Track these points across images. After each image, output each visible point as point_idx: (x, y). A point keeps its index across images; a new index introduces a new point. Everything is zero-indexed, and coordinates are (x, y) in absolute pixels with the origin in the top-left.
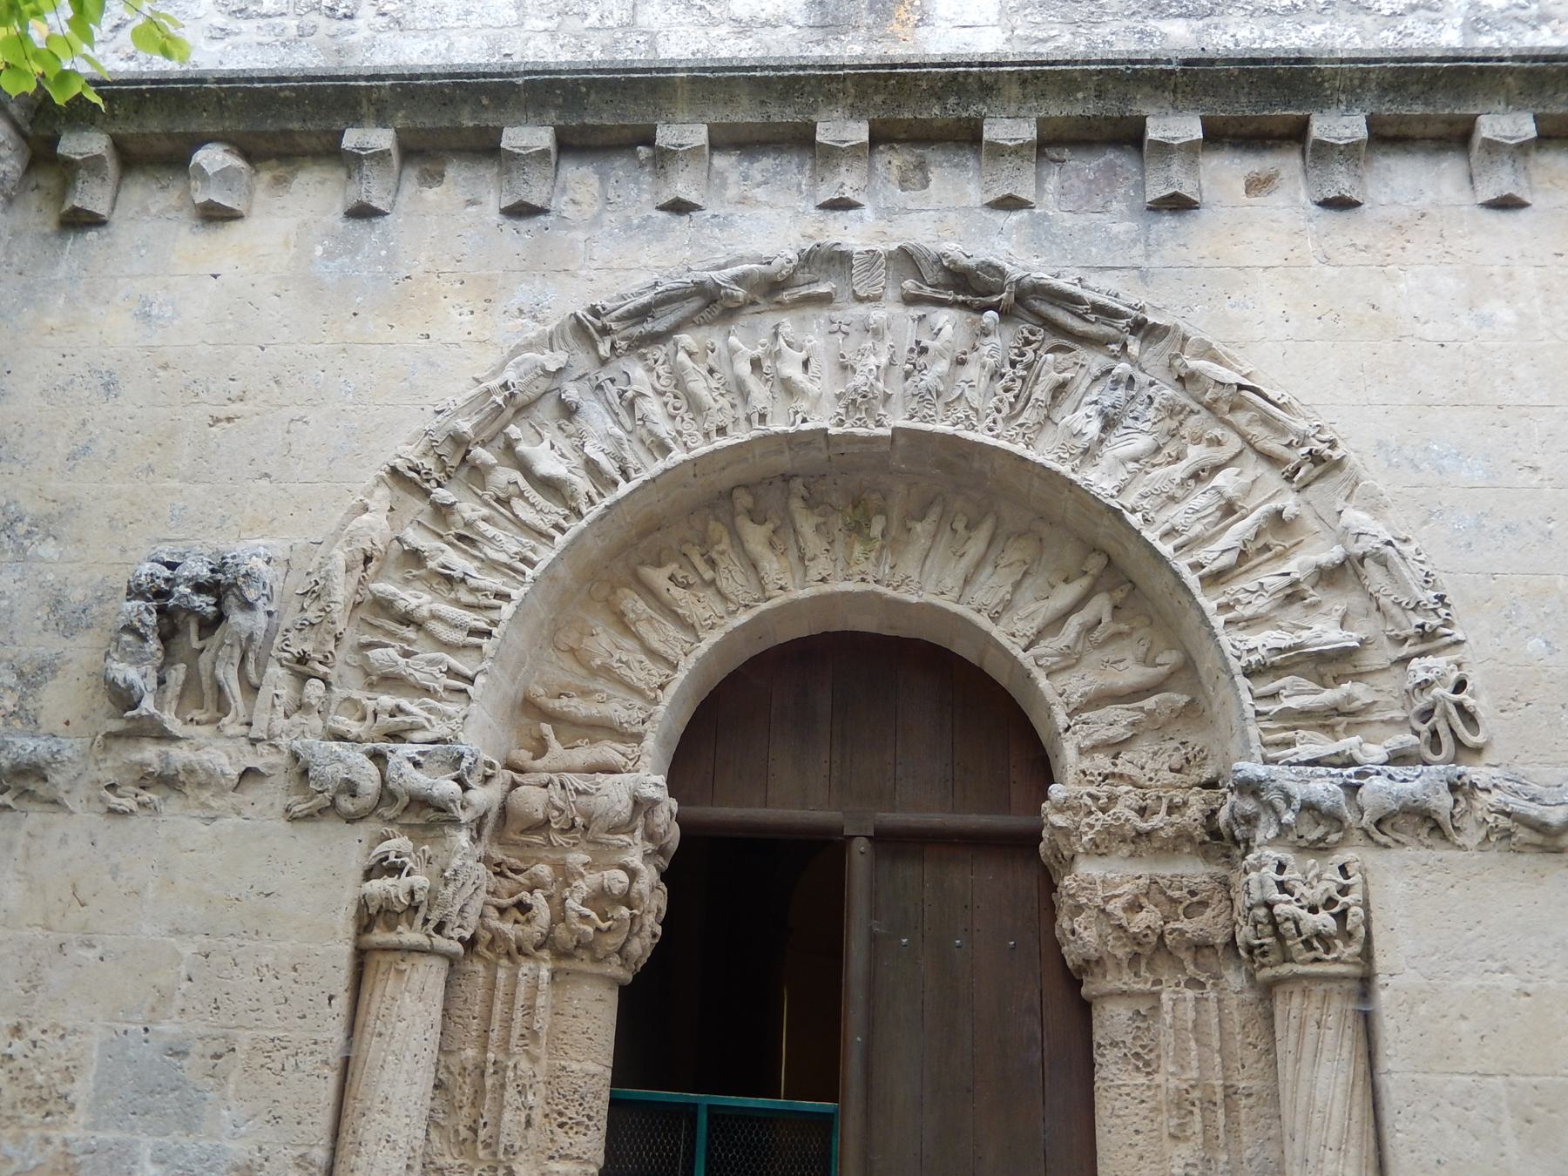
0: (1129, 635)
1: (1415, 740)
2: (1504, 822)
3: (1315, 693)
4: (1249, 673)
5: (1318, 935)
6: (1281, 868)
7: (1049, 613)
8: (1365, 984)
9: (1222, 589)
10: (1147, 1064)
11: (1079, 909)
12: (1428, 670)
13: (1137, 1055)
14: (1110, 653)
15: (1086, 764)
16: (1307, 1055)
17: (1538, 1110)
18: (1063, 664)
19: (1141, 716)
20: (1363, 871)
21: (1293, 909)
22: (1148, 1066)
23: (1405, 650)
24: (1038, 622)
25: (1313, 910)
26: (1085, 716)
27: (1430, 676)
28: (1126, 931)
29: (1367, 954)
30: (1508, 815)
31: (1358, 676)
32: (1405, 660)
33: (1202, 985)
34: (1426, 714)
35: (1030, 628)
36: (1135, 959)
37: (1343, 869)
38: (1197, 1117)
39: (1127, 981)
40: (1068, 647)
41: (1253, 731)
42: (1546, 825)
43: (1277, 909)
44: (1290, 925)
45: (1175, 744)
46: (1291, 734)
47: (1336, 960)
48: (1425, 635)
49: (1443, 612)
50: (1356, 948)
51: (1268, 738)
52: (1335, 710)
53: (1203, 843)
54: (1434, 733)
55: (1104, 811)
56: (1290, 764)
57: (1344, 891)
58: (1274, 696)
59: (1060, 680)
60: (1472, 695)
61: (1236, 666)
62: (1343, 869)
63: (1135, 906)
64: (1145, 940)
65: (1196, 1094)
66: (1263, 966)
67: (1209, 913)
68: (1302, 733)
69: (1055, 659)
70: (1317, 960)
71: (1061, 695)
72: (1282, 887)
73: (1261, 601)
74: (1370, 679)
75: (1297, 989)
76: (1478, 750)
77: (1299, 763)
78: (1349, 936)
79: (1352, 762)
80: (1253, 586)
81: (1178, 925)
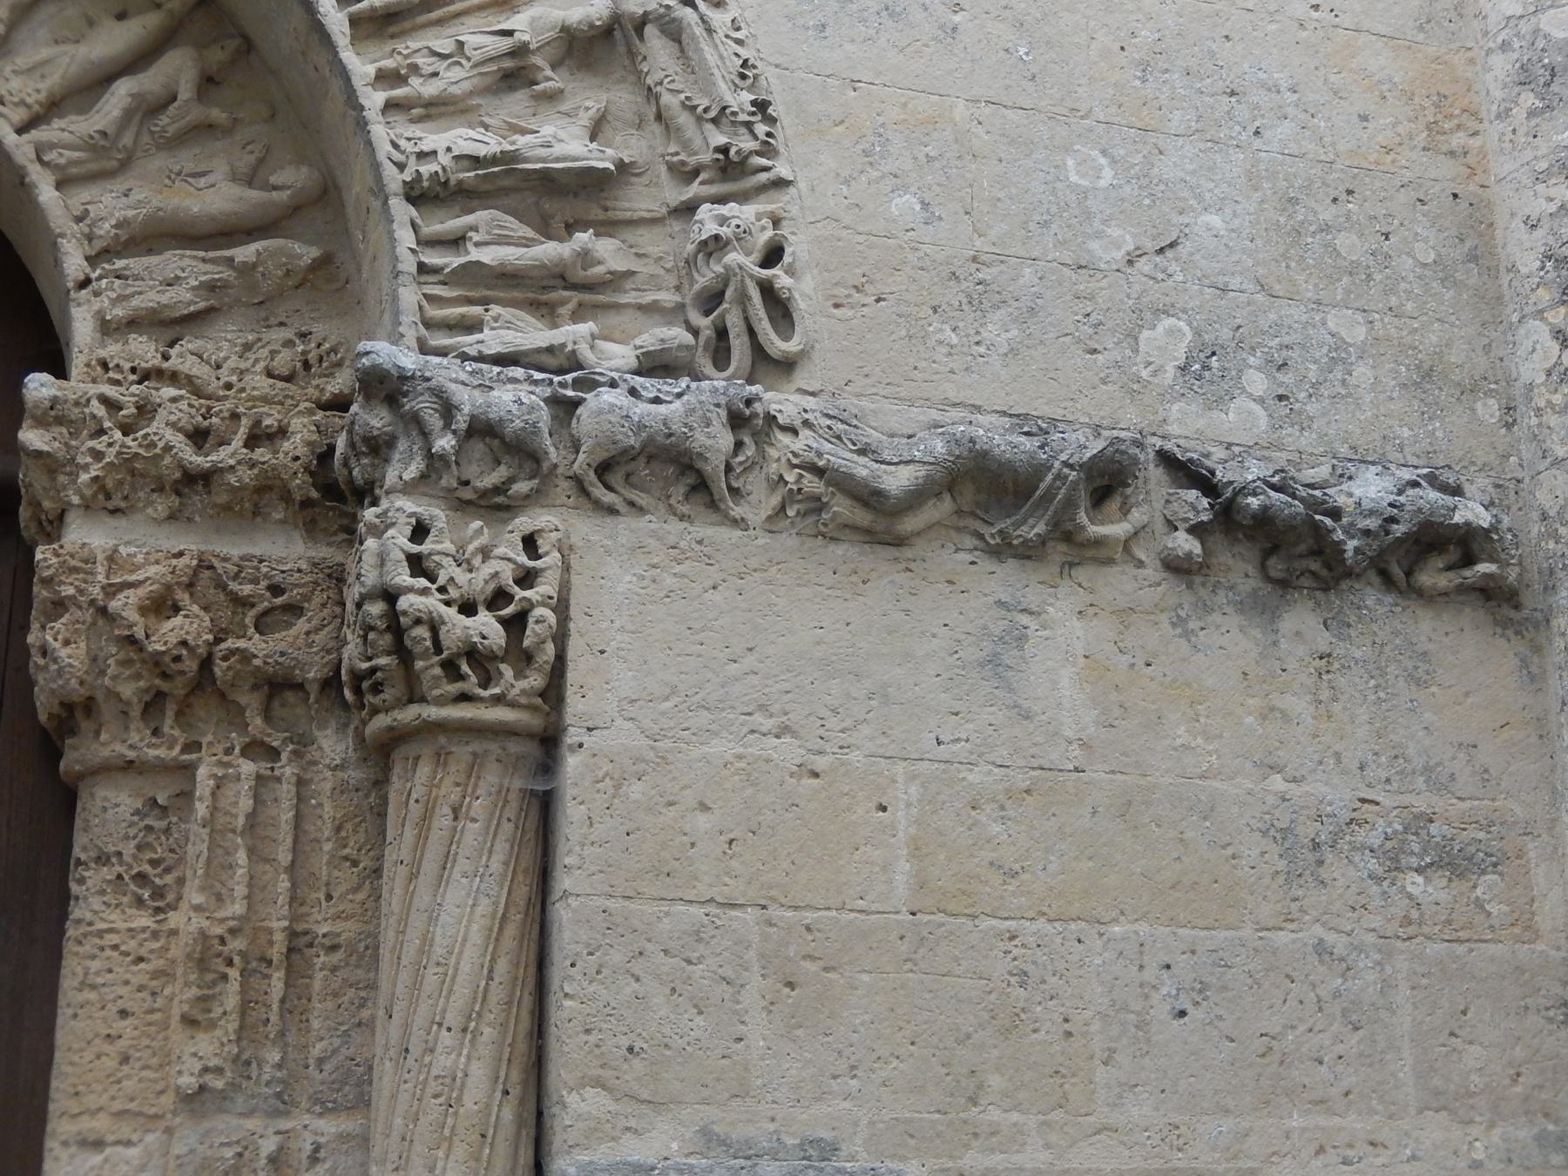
0: (228, 130)
1: (688, 338)
2: (812, 484)
3: (527, 243)
4: (417, 195)
5: (472, 653)
6: (420, 532)
7: (74, 69)
9: (389, 46)
10: (158, 893)
11: (59, 606)
12: (723, 221)
13: (141, 878)
14: (185, 159)
15: (112, 350)
16: (429, 867)
17: (807, 964)
18: (93, 167)
19: (227, 274)
20: (565, 550)
21: (432, 603)
22: (160, 901)
23: (695, 189)
24: (52, 81)
25: (468, 609)
26: (120, 264)
27: (724, 231)
28: (141, 650)
29: (553, 692)
30: (819, 472)
31: (607, 227)
33: (274, 754)
34: (711, 300)
35: (35, 91)
36: (154, 704)
37: (530, 543)
38: (234, 986)
39: (136, 742)
40: (104, 134)
41: (409, 296)
42: (878, 493)
43: (403, 603)
44: (422, 632)
45: (287, 333)
46: (477, 310)
47: (498, 700)
48: (729, 166)
49: (761, 129)
50: (535, 680)
51: (435, 313)
53: (307, 504)
54: (722, 333)
55: (126, 430)
56: (464, 357)
57: (527, 578)
58: (456, 242)
59: (81, 196)
60: (790, 272)
61: (394, 179)
62: (530, 543)
63: (162, 605)
64: (176, 667)
65: (237, 944)
66: (375, 711)
67: (302, 625)
68: (496, 309)
69: (76, 155)
70: (464, 698)
71: (79, 220)
72: (417, 564)
73: (456, 73)
74: (631, 235)
75: (427, 752)
76: (787, 366)
77: (481, 358)
78: (525, 659)
79: (575, 363)
80: (444, 45)
81: (241, 644)
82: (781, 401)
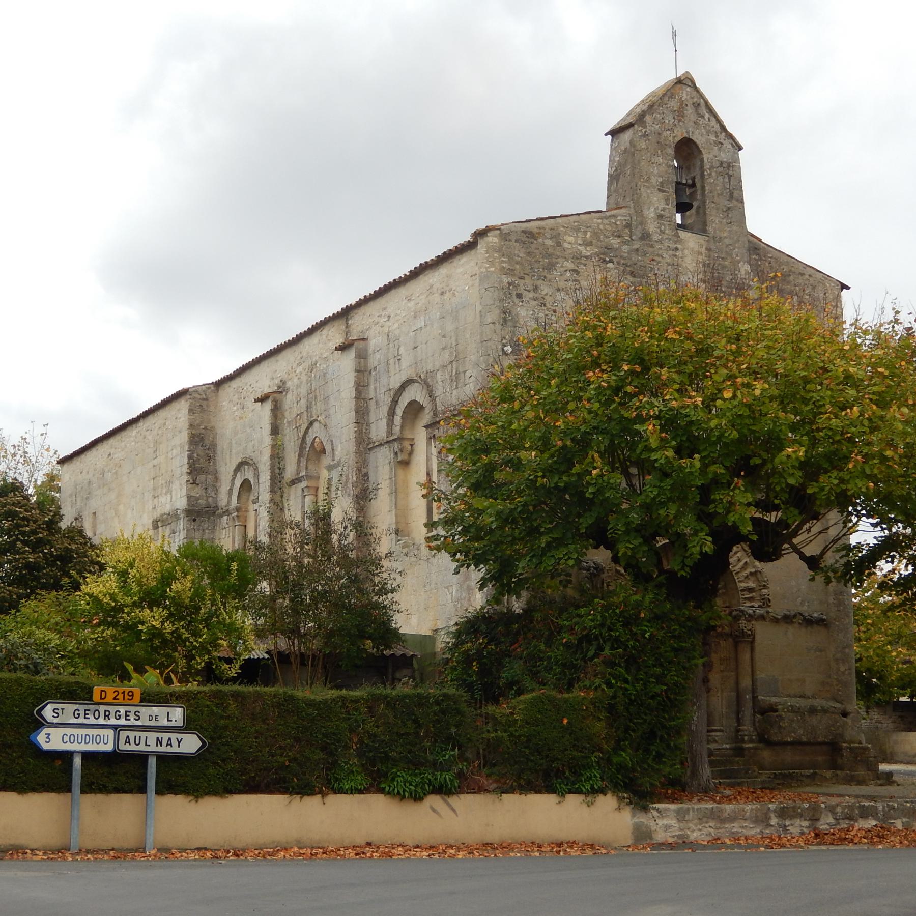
4: (741, 591)
8: (753, 642)
29: (754, 638)
31: (754, 592)
32: (761, 590)
48: (765, 586)
52: (752, 598)
82: (770, 610)
